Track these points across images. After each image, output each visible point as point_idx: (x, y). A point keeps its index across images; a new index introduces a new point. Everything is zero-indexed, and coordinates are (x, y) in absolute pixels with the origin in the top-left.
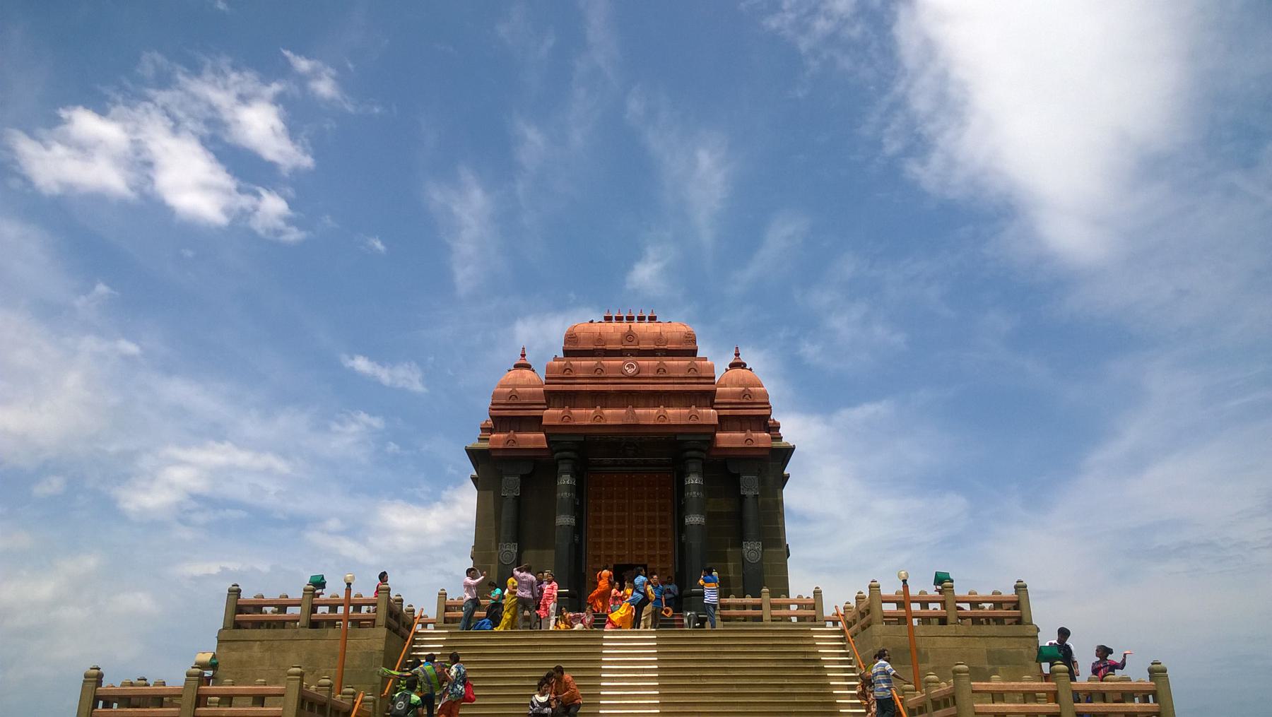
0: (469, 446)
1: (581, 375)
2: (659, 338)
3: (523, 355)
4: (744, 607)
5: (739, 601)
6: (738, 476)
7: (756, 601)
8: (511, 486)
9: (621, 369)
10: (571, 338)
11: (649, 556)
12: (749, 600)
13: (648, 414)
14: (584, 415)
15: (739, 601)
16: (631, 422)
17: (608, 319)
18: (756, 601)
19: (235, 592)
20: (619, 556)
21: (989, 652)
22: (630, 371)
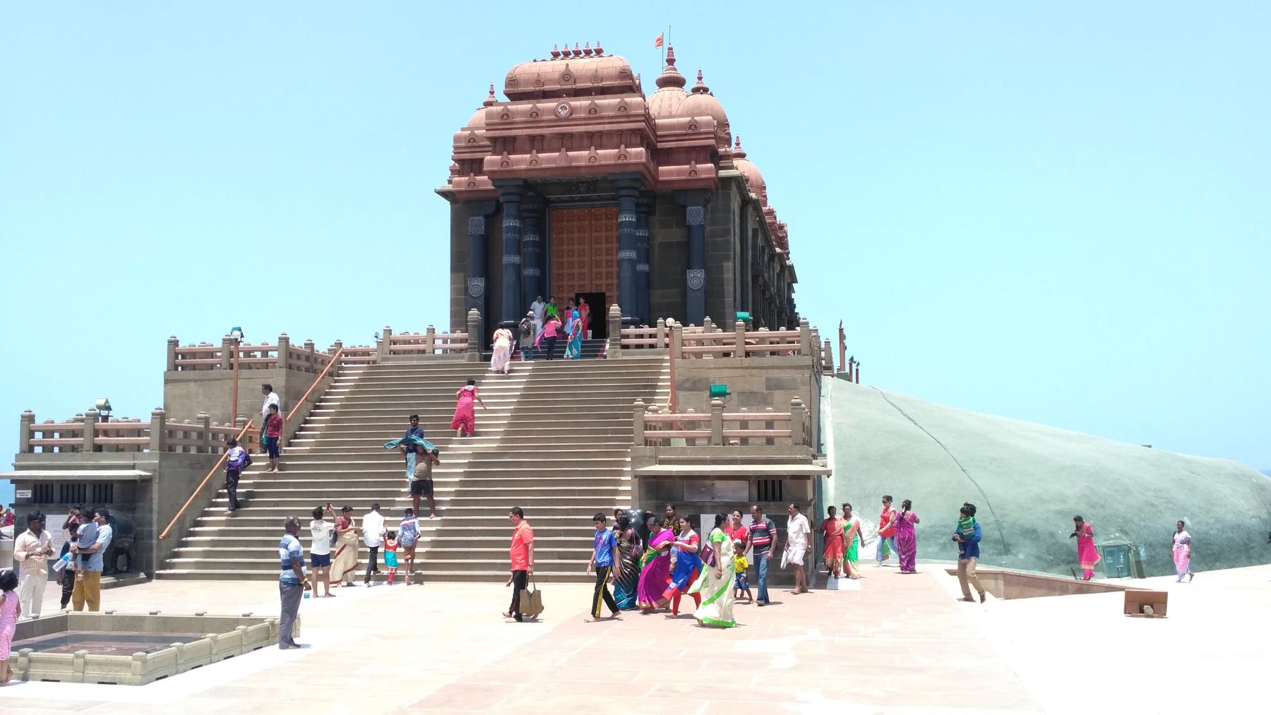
0: (439, 188)
1: (518, 119)
2: (596, 77)
3: (492, 93)
4: (641, 336)
5: (638, 331)
6: (684, 207)
7: (653, 330)
8: (477, 224)
9: (554, 112)
10: (512, 81)
11: (608, 285)
12: (646, 330)
13: (581, 156)
14: (521, 161)
15: (638, 331)
16: (563, 164)
17: (556, 55)
18: (653, 330)
19: (174, 343)
20: (580, 286)
21: (767, 379)
22: (563, 113)
